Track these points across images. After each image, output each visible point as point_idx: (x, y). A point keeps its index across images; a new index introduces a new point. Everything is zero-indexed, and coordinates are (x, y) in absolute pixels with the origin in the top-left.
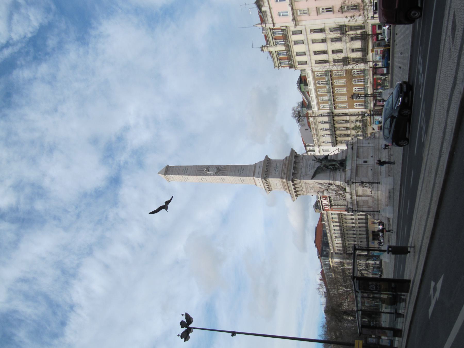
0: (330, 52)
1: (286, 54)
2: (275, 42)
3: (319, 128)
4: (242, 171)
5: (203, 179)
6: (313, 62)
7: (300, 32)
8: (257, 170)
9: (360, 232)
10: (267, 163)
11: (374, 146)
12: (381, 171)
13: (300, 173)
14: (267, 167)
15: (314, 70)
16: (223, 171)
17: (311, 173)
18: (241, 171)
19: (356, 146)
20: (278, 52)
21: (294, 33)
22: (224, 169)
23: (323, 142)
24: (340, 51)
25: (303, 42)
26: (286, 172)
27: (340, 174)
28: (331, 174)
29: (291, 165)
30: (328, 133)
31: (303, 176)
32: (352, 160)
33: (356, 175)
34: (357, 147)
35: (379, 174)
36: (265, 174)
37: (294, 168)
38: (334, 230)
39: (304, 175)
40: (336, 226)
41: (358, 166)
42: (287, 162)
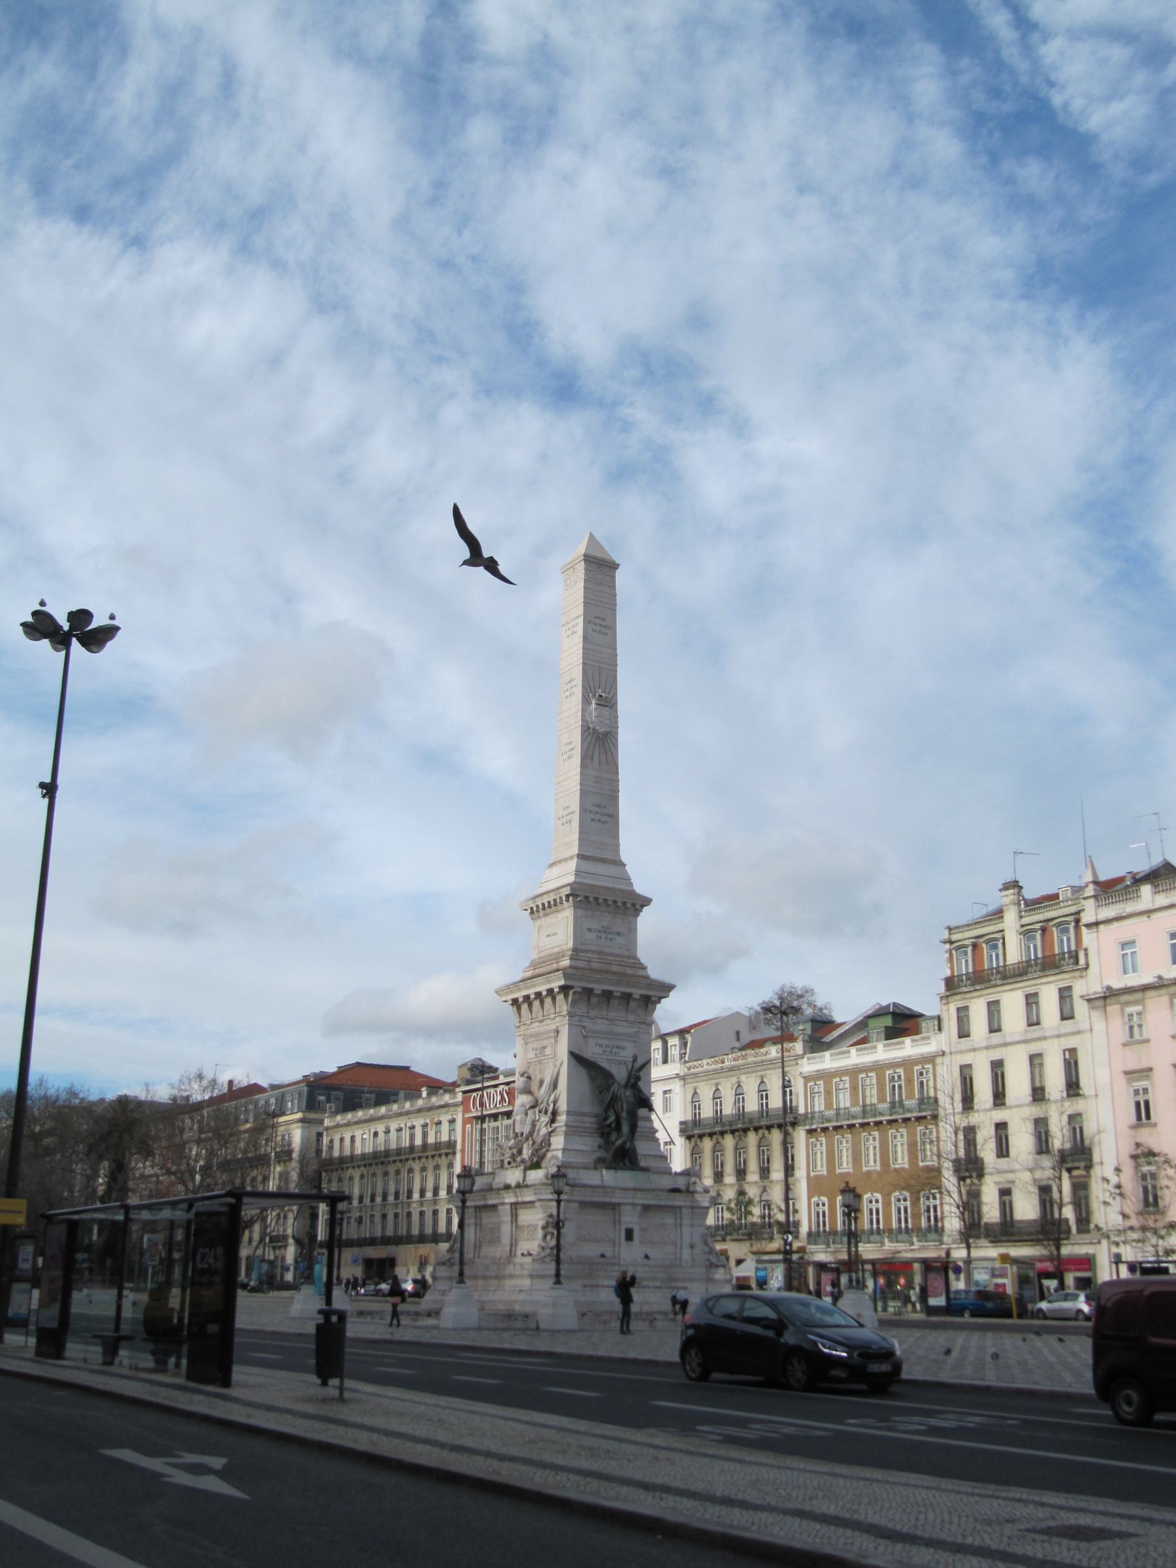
0: (999, 1115)
1: (993, 968)
2: (1034, 931)
3: (743, 1078)
4: (597, 817)
5: (572, 688)
6: (967, 1059)
7: (1067, 1015)
8: (601, 869)
9: (390, 1217)
10: (624, 903)
11: (684, 1264)
12: (597, 1286)
13: (592, 1013)
14: (610, 903)
15: (939, 1060)
17: (592, 1051)
18: (597, 813)
19: (682, 1204)
20: (1001, 941)
21: (1065, 994)
23: (695, 1090)
24: (1003, 1150)
25: (1033, 1022)
26: (594, 965)
27: (584, 1148)
28: (586, 1119)
30: (728, 1109)
31: (584, 1024)
32: (635, 1190)
33: (584, 1205)
34: (680, 1207)
35: (586, 1282)
36: (588, 895)
37: (608, 995)
38: (399, 1130)
39: (584, 1027)
40: (412, 1137)
41: (614, 1209)
42: (629, 971)
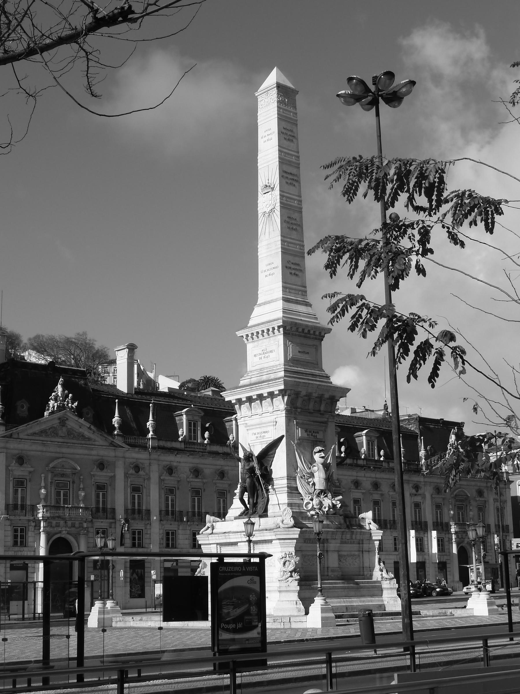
16: (267, 231)
18: (268, 270)
22: (272, 227)
29: (252, 391)
31: (246, 422)
